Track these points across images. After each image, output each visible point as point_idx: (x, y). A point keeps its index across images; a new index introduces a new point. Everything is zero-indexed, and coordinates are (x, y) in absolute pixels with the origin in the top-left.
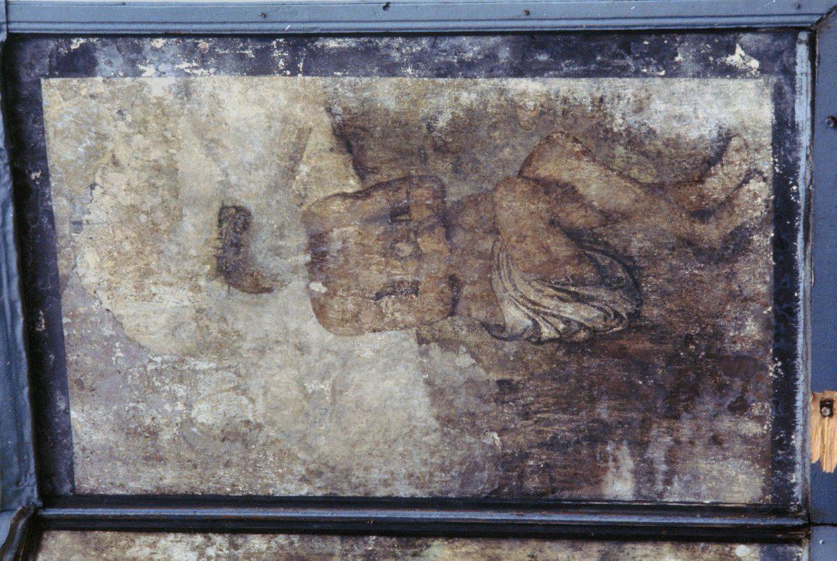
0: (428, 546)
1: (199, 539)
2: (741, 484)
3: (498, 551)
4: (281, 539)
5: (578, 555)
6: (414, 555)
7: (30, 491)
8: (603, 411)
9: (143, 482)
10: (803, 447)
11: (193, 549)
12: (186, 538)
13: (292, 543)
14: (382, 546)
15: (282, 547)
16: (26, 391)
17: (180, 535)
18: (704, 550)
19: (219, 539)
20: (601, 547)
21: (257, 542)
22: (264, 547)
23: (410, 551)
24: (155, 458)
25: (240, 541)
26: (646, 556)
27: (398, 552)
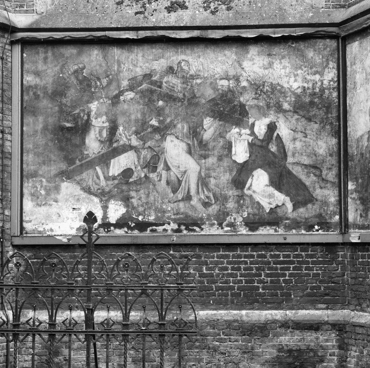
0: (335, 138)
1: (336, 79)
2: (351, 216)
3: (334, 156)
4: (337, 100)
5: (334, 176)
6: (332, 135)
7: (343, 34)
8: (360, 181)
9: (348, 63)
10: (355, 232)
11: (332, 78)
12: (336, 76)
13: (335, 103)
14: (335, 126)
15: (334, 101)
16: (356, 30)
17: (337, 74)
18: (337, 208)
19: (336, 84)
20: (337, 182)
21: (335, 94)
22: (334, 96)
23: (333, 134)
24: (351, 65)
25: (335, 90)
26: (334, 193)
27: (334, 131)
